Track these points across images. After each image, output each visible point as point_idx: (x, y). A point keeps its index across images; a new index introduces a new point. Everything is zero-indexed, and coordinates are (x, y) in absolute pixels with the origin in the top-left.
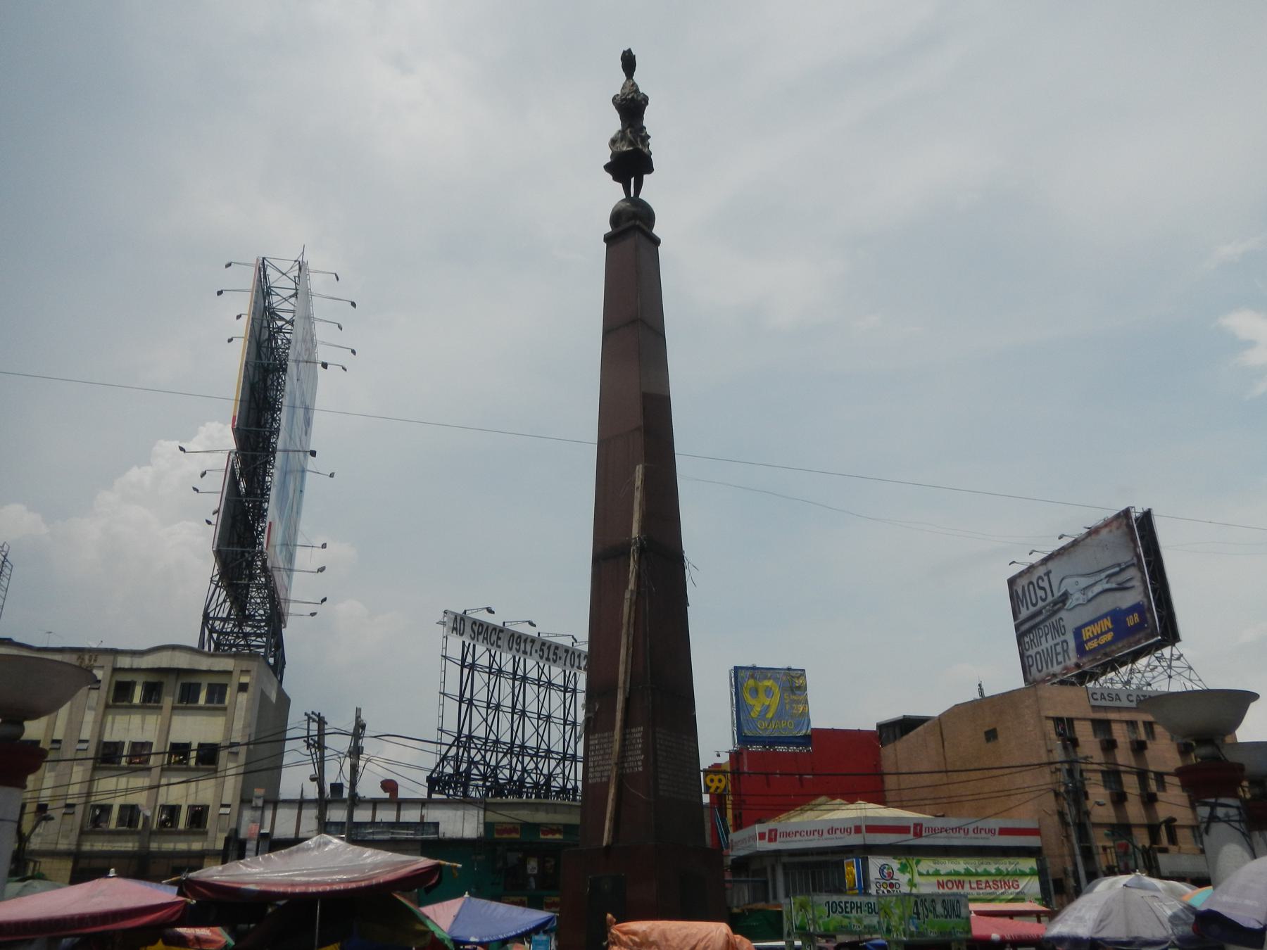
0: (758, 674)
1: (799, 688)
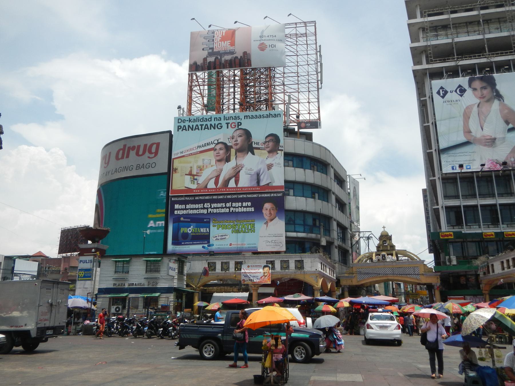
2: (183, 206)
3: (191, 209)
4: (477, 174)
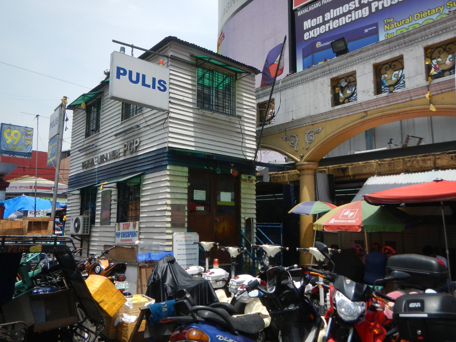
0: (12, 127)
1: (30, 135)
2: (320, 19)
3: (334, 19)
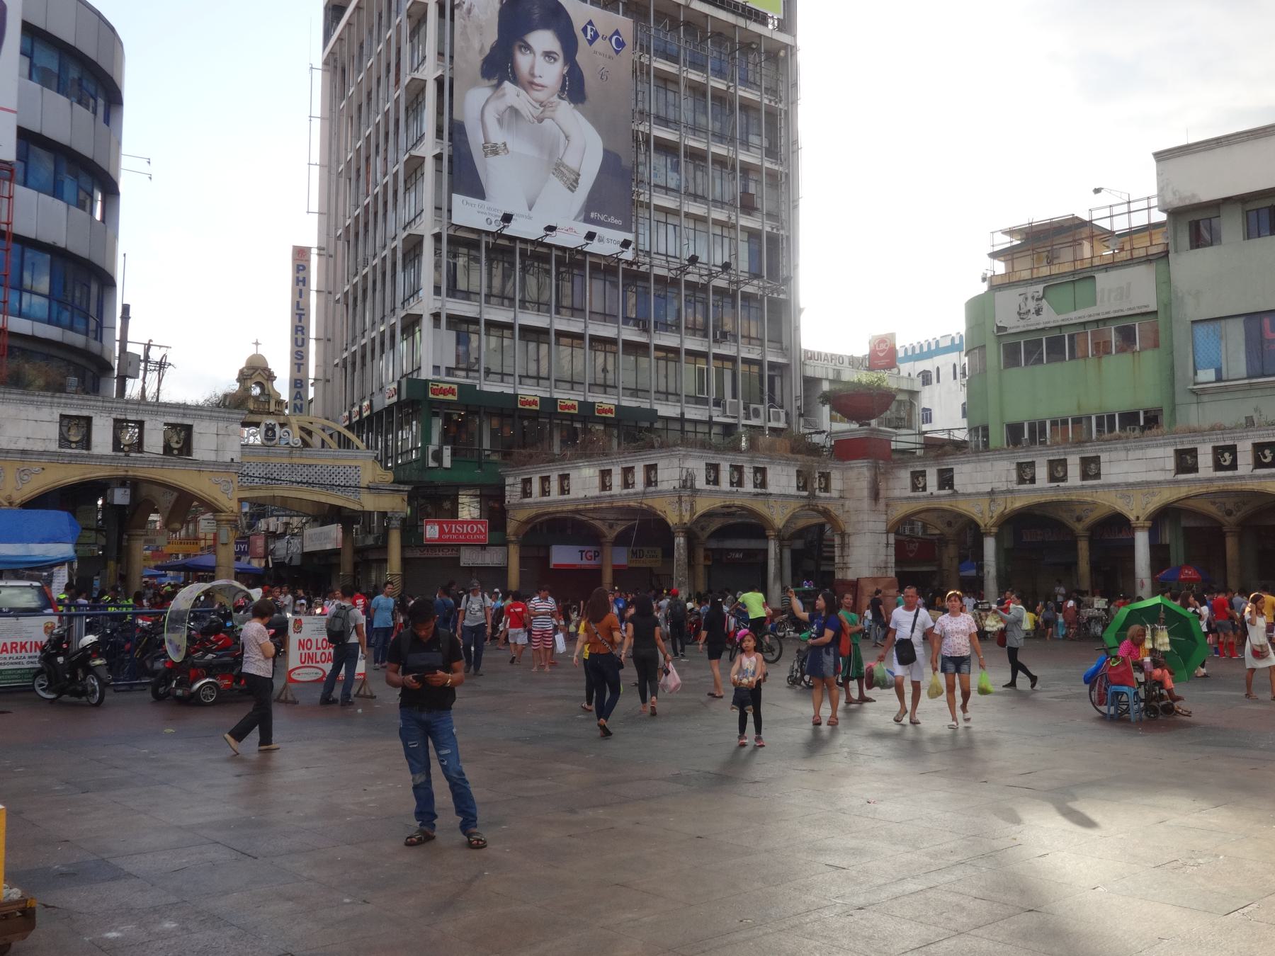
4: (523, 246)
